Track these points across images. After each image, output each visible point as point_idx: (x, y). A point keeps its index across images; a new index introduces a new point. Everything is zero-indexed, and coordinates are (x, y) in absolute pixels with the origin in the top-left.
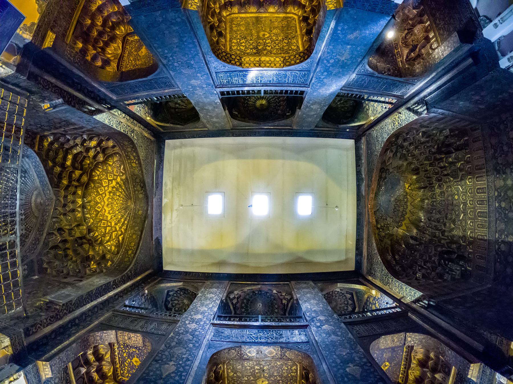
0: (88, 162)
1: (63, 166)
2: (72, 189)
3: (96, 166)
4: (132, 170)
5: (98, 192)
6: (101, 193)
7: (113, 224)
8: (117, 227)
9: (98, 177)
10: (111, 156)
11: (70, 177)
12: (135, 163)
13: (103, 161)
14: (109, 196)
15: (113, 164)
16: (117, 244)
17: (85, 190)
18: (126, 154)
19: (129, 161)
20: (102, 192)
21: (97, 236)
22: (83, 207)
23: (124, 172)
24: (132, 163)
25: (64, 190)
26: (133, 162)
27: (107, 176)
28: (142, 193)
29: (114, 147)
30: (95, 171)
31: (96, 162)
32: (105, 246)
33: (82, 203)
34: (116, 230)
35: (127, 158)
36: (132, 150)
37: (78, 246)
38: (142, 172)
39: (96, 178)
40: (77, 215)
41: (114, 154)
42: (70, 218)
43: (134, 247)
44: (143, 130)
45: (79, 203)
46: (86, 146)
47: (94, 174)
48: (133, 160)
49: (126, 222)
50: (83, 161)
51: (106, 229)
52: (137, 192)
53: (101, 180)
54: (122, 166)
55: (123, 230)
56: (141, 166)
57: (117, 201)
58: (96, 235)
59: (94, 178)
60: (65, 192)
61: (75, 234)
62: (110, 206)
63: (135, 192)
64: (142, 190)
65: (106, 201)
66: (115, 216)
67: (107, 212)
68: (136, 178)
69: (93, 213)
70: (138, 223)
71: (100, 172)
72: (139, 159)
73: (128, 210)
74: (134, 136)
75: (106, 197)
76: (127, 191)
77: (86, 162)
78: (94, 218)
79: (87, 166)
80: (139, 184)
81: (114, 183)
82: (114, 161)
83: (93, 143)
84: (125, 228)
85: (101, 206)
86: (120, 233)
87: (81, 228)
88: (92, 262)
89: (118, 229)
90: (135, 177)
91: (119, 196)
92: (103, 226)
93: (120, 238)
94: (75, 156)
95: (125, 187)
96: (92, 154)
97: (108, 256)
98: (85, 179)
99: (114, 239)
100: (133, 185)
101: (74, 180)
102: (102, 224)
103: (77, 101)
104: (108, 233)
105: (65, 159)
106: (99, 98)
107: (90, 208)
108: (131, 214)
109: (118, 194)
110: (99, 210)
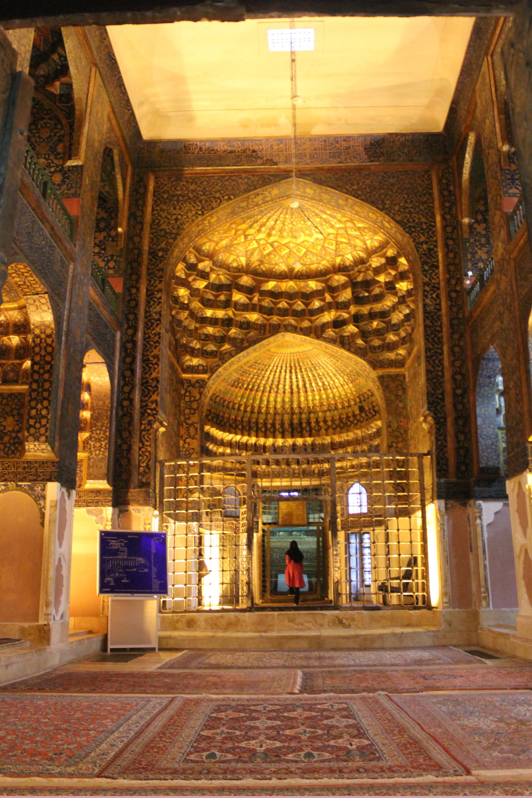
1: (228, 323)
7: (331, 231)
8: (338, 226)
9: (242, 256)
15: (213, 241)
26: (209, 223)
30: (231, 263)
31: (214, 268)
34: (345, 229)
47: (235, 265)
49: (328, 212)
51: (342, 242)
53: (247, 251)
55: (344, 219)
62: (296, 234)
63: (267, 202)
66: (316, 227)
67: (308, 238)
69: (310, 259)
75: (279, 241)
77: (215, 279)
78: (319, 258)
83: (183, 292)
89: (342, 225)
94: (207, 304)
98: (246, 280)
100: (253, 207)
101: (251, 299)
102: (331, 247)
103: (147, 399)
104: (349, 240)
105: (214, 322)
106: (128, 360)
110: (304, 250)
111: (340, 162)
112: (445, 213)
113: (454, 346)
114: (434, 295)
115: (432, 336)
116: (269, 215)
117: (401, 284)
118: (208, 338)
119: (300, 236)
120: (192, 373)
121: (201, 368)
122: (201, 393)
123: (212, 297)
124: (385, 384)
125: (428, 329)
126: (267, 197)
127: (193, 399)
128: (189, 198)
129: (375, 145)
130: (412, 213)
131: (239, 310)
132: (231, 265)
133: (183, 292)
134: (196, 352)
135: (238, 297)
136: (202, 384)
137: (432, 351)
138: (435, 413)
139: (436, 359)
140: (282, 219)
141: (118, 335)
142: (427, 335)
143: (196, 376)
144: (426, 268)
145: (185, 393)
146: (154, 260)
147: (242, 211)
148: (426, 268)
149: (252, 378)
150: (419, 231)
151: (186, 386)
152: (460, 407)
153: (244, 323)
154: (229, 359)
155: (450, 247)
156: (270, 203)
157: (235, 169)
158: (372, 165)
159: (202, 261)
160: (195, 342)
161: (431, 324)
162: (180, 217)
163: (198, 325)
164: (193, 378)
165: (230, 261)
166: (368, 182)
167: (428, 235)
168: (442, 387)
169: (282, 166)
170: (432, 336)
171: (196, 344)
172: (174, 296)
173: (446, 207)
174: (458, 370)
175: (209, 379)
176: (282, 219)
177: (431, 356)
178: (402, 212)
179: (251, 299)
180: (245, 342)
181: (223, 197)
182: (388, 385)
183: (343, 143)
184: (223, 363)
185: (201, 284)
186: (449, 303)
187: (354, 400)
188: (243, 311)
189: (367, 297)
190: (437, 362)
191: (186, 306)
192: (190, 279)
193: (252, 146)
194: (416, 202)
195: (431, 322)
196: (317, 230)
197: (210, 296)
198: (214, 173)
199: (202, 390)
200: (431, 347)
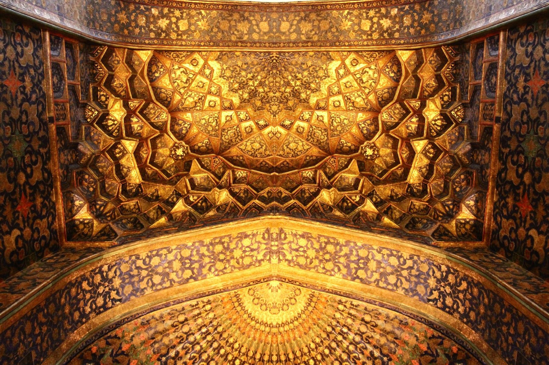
12: (178, 19)
24: (178, 27)
26: (176, 23)
31: (172, 136)
36: (142, 13)
68: (218, 28)
80: (233, 23)
90: (215, 30)
156: (258, 45)
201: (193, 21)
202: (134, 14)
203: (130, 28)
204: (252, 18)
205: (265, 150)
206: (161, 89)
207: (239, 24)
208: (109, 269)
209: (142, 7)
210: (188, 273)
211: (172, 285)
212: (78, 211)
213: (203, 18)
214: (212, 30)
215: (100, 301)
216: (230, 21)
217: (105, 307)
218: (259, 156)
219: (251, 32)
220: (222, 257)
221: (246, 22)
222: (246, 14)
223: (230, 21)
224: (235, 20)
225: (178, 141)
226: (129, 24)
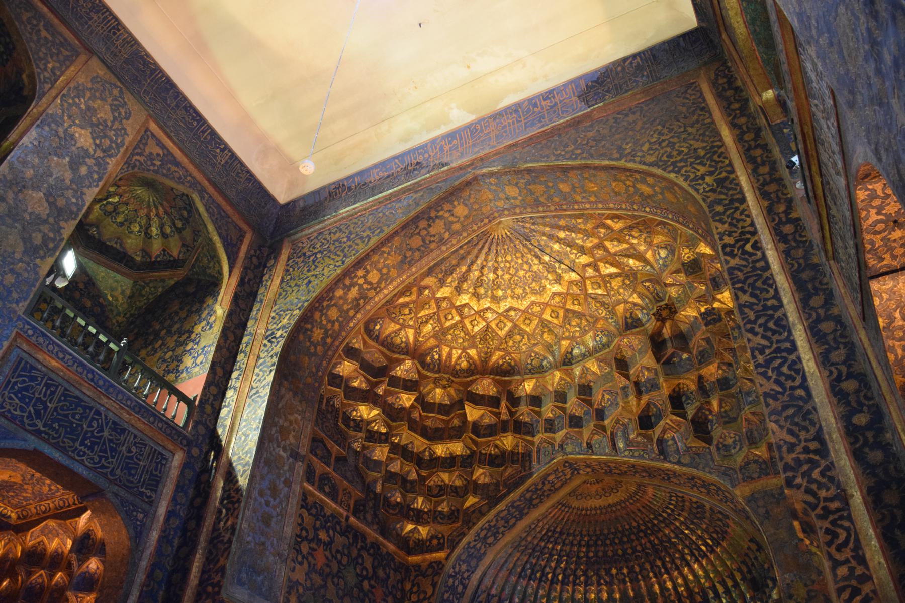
0: (438, 390)
2: (524, 412)
3: (441, 367)
4: (393, 273)
5: (510, 334)
6: (509, 325)
8: (589, 245)
9: (470, 348)
10: (388, 344)
11: (492, 431)
12: (364, 276)
13: (413, 358)
14: (509, 299)
15: (410, 327)
16: (640, 231)
17: (519, 373)
18: (352, 313)
19: (372, 293)
20: (506, 321)
21: (641, 296)
22: (567, 361)
23: (415, 289)
24: (370, 283)
25: (533, 436)
26: (366, 282)
27: (454, 326)
28: (450, 211)
29: (351, 353)
30: (456, 364)
31: (429, 374)
32: (662, 270)
33: (557, 368)
34: (600, 246)
35: (365, 304)
36: (329, 307)
37: (686, 349)
38: (383, 243)
39: (473, 352)
40: (594, 373)
41: (376, 339)
42: (607, 396)
43: (624, 182)
44: (261, 301)
45: (561, 379)
46: (388, 426)
47: (464, 364)
48: (361, 286)
49: (562, 223)
50: (442, 409)
51: (611, 276)
52: (456, 227)
54: (401, 300)
56: (367, 256)
57: (512, 271)
58: (639, 301)
59: (476, 357)
60: (538, 432)
61: (648, 369)
63: (458, 233)
64: (437, 217)
65: (525, 304)
66: (561, 262)
67: (557, 288)
69: (578, 325)
70: (547, 187)
71: (452, 348)
72: (347, 273)
73: (524, 227)
74: (284, 327)
75: (516, 305)
76: (469, 253)
78: (591, 320)
79: (452, 391)
80: (424, 233)
81: (464, 299)
82: (398, 327)
83: (366, 412)
84: (579, 221)
85: (548, 311)
86: (603, 231)
87: (628, 354)
88: (716, 305)
89: (596, 241)
90: (409, 254)
91: (495, 270)
92: (603, 288)
93: (617, 226)
94: (436, 435)
95: (458, 265)
96: (404, 396)
97: (686, 254)
98: (485, 386)
99: (628, 242)
101: (497, 415)
102: (599, 291)
105: (450, 462)
107: (563, 339)
108: (531, 218)
109: (492, 276)
111: (542, 126)
112: (735, 117)
113: (818, 320)
114: (748, 247)
115: (761, 321)
116: (479, 262)
117: (719, 296)
118: (443, 489)
119: (544, 288)
120: (422, 552)
121: (435, 542)
122: (434, 585)
123: (441, 425)
124: (762, 511)
125: (746, 310)
126: (452, 223)
127: (422, 597)
128: (330, 251)
129: (594, 87)
130: (674, 143)
131: (484, 436)
132: (458, 367)
133: (366, 412)
134: (425, 516)
135: (473, 413)
136: (438, 567)
137: (767, 352)
138: (808, 491)
139: (781, 365)
140: (502, 265)
141: (177, 460)
142: (749, 322)
143: (428, 556)
144: (720, 209)
145: (411, 589)
146: (269, 344)
147: (421, 257)
148: (720, 209)
149: (558, 562)
150: (692, 163)
151: (414, 574)
152: (876, 456)
153: (497, 457)
154: (478, 520)
155: (759, 159)
157: (391, 194)
158: (592, 111)
159: (400, 362)
160: (420, 500)
161: (753, 300)
162: (312, 279)
163: (424, 473)
164: (424, 560)
165: (454, 360)
166: (590, 134)
167: (712, 160)
168: (813, 423)
169: (454, 165)
170: (761, 321)
171: (419, 502)
172: (354, 420)
173: (734, 110)
174: (844, 369)
175: (447, 558)
176: (502, 265)
177: (767, 363)
178: (656, 149)
179: (497, 415)
180: (501, 488)
181: (373, 233)
182: (767, 512)
183: (544, 103)
184: (469, 528)
185: (406, 399)
186: (782, 246)
187: (739, 570)
188: (490, 436)
189: (689, 359)
190: (785, 369)
191: (383, 437)
192: (380, 391)
193: (415, 159)
194: (680, 127)
195: (753, 295)
196: (563, 266)
197: (433, 420)
198: (365, 210)
199: (436, 579)
200: (765, 343)
201: (380, 265)
202: (323, 318)
203: (330, 332)
204: (441, 213)
205: (529, 339)
206: (389, 335)
207: (431, 230)
208: (454, 568)
209: (325, 303)
210: (513, 521)
211: (503, 535)
212: (402, 529)
213: (389, 253)
214: (405, 257)
215: (460, 588)
216: (419, 234)
217: (465, 587)
218: (524, 348)
219: (448, 226)
220: (534, 497)
221: (437, 221)
222: (433, 214)
223: (419, 234)
224: (424, 229)
225: (437, 375)
226: (326, 332)
